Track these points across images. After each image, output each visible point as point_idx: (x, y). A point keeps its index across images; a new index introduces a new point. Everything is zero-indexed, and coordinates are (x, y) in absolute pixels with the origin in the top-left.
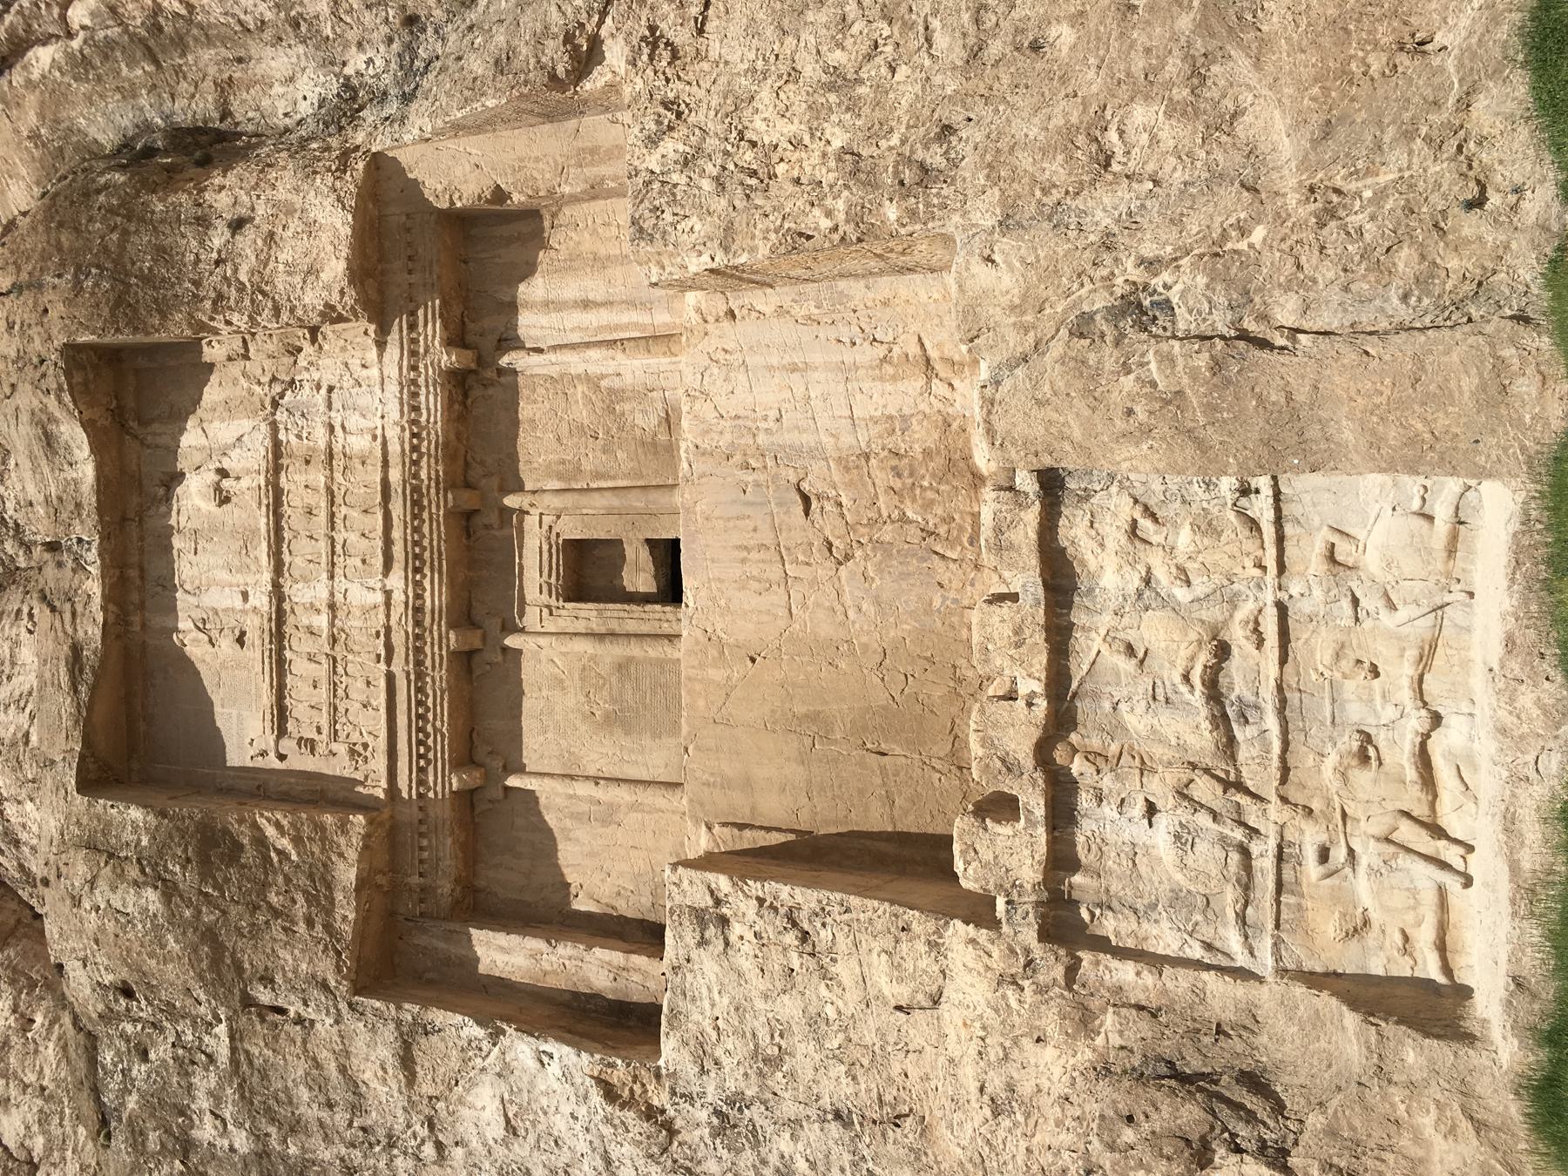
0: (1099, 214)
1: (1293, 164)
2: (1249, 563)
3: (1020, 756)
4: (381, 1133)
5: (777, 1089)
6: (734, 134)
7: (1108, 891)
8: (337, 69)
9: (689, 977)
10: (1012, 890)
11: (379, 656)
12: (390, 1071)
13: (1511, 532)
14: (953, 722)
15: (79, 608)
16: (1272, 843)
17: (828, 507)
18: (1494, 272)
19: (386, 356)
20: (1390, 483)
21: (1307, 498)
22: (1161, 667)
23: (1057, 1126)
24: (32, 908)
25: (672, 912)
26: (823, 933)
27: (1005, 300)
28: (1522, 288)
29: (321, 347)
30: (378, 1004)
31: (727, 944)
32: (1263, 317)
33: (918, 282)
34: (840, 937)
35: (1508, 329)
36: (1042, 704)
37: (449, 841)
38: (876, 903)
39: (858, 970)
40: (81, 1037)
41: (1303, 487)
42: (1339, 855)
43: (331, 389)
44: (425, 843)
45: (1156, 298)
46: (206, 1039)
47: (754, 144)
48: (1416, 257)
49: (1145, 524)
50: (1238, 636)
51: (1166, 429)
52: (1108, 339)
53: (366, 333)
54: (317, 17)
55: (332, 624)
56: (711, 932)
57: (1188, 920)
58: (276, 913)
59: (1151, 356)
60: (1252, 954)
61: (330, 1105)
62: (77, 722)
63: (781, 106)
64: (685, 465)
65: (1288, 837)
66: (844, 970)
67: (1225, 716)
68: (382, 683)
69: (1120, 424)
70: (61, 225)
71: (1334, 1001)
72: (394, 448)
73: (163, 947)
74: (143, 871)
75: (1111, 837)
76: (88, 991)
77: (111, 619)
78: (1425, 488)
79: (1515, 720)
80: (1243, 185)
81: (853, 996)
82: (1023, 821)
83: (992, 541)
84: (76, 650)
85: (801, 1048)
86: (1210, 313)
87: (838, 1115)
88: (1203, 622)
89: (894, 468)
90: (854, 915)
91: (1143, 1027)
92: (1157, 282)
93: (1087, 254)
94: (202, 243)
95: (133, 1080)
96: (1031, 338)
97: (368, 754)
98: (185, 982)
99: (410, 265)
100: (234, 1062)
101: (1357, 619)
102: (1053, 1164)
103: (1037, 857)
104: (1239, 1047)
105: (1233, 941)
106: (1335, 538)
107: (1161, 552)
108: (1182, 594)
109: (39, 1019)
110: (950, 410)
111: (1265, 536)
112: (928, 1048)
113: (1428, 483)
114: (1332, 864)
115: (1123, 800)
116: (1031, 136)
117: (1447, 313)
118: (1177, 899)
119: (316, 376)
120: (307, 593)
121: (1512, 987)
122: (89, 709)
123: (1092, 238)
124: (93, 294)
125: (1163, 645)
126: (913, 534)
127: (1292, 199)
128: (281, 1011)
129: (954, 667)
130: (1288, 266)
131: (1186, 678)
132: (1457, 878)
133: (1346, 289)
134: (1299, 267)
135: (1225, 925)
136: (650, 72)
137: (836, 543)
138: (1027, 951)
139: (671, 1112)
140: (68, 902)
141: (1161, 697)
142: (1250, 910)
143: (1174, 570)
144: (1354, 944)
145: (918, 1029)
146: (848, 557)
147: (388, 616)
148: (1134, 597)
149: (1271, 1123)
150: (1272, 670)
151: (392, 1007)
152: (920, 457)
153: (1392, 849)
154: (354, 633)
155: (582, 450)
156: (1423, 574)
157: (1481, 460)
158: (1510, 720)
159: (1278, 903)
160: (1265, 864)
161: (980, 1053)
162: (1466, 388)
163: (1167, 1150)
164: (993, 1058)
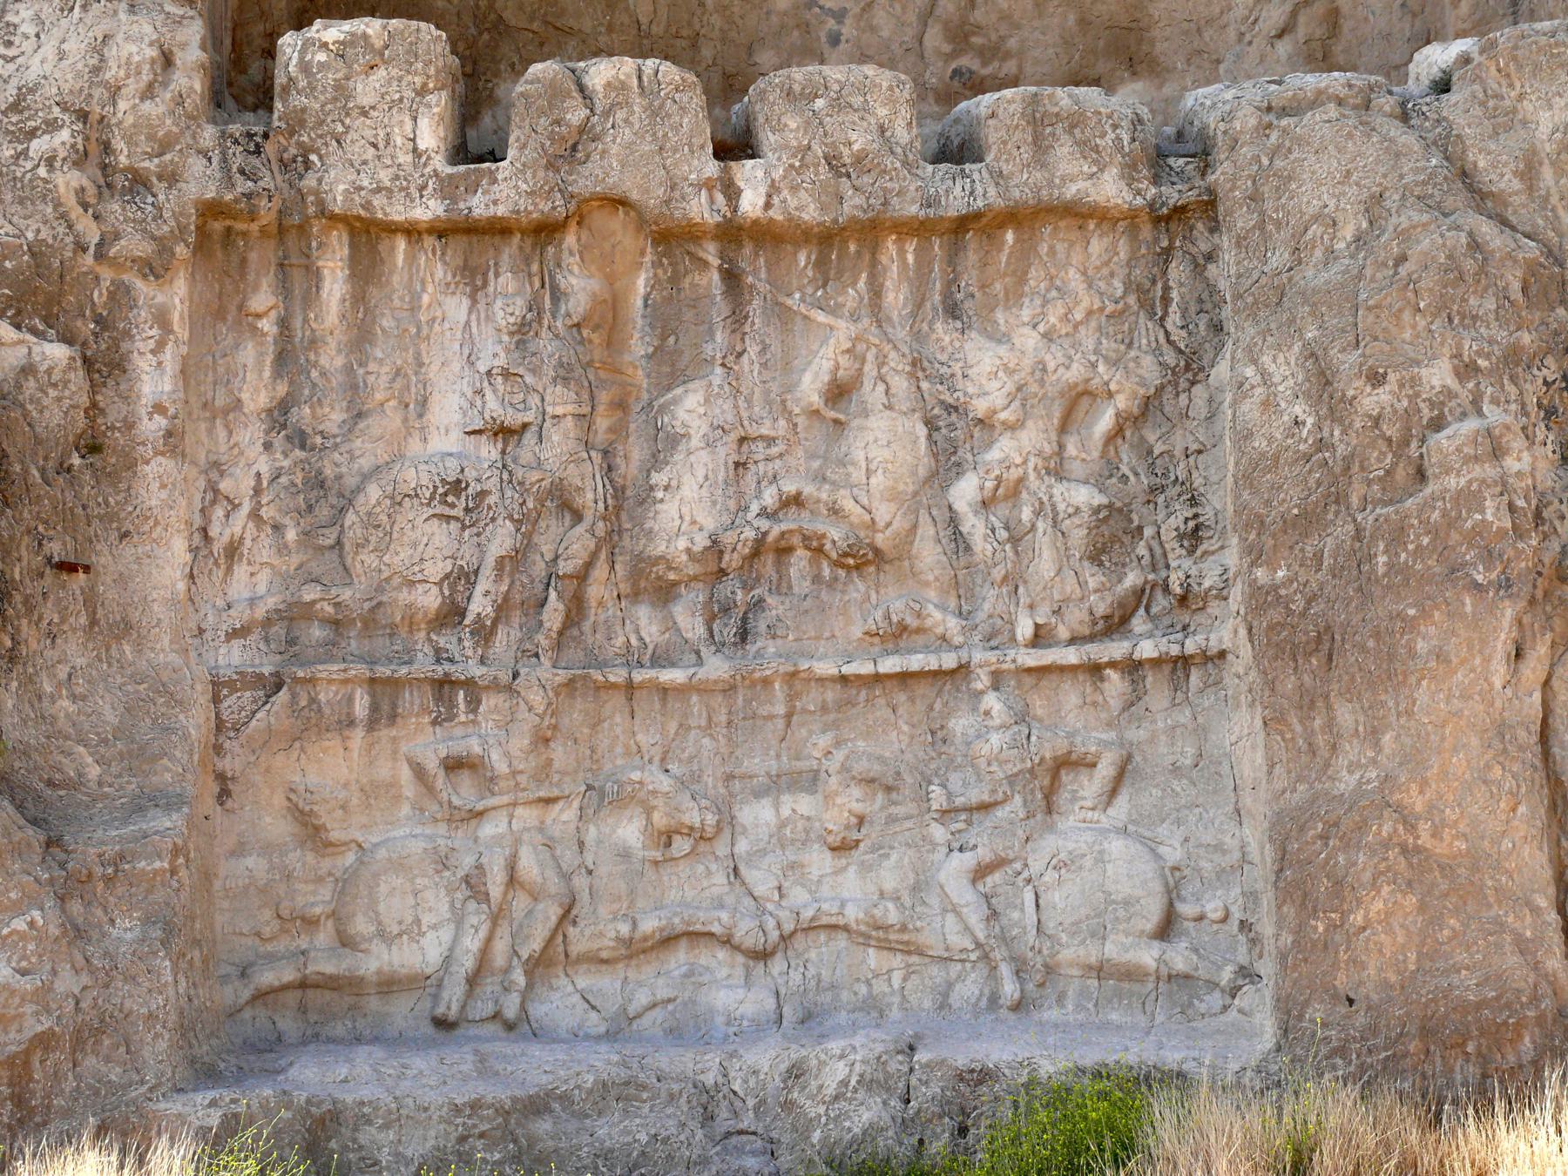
3: (594, 167)
21: (1184, 716)
42: (465, 793)
51: (1341, 450)
79: (830, 1090)
82: (450, 170)
106: (1106, 769)
143: (1015, 474)
156: (1050, 926)
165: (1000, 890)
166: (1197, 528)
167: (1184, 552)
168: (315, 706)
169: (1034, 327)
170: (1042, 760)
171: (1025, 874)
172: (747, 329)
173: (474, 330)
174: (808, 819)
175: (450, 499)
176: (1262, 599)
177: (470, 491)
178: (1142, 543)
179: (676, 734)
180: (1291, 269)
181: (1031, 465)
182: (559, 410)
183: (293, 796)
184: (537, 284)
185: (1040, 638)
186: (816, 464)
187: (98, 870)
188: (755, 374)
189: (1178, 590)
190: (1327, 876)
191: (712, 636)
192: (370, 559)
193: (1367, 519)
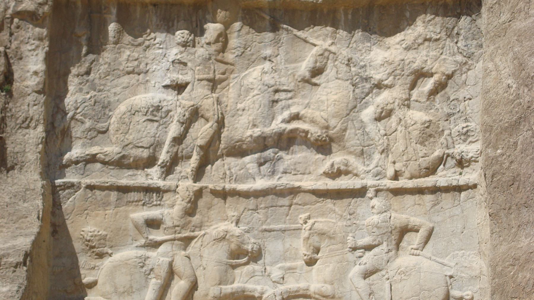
2: (398, 166)
16: (161, 183)
20: (474, 274)
21: (457, 211)
22: (304, 97)
49: (429, 84)
51: (527, 99)
57: (84, 115)
65: (166, 196)
67: (265, 148)
71: (36, 230)
75: (151, 53)
88: (345, 130)
101: (354, 249)
106: (423, 232)
107: (404, 97)
111: (422, 180)
114: (144, 229)
115: (185, 64)
125: (324, 98)
131: (296, 117)
135: (84, 145)
141: (277, 96)
142: (98, 165)
143: (389, 107)
150: (307, 183)
165: (375, 282)
166: (467, 131)
167: (461, 141)
168: (94, 197)
169: (401, 45)
170: (396, 228)
171: (386, 276)
172: (279, 45)
173: (168, 44)
174: (297, 249)
175: (155, 113)
176: (491, 162)
177: (163, 110)
178: (443, 137)
179: (243, 212)
180: (510, 21)
181: (396, 104)
182: (201, 76)
183: (82, 233)
184: (194, 25)
185: (396, 176)
188: (283, 64)
189: (458, 158)
190: (514, 282)
191: (260, 172)
192: (121, 137)
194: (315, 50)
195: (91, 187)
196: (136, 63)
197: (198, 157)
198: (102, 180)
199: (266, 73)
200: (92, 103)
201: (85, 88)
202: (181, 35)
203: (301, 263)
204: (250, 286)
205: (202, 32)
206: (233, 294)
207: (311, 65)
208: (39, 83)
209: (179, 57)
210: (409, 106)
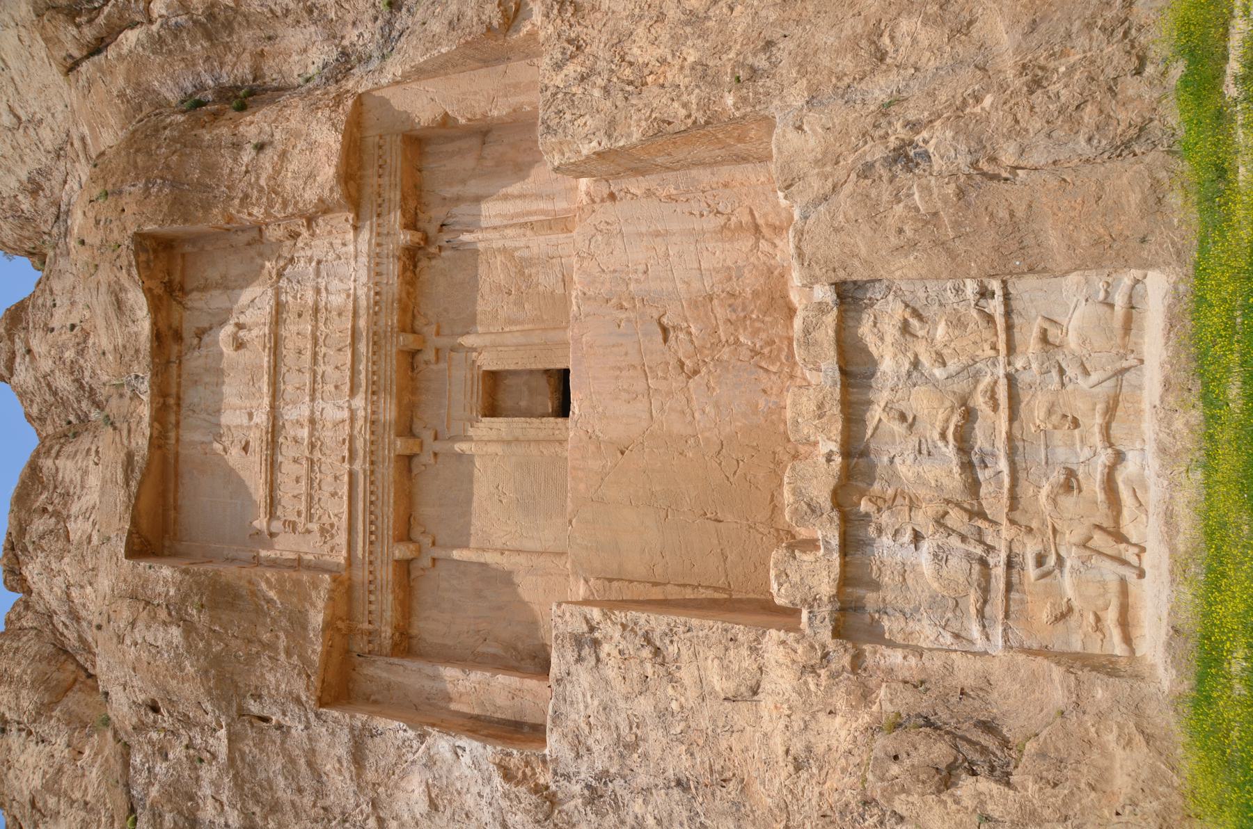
0: (877, 92)
1: (1010, 52)
2: (987, 347)
3: (821, 500)
4: (337, 811)
5: (634, 766)
6: (618, 57)
7: (884, 600)
8: (337, 41)
9: (569, 687)
10: (812, 602)
11: (344, 458)
12: (345, 764)
13: (1166, 304)
14: (773, 495)
15: (133, 426)
16: (1003, 556)
17: (682, 336)
18: (1151, 120)
19: (360, 240)
20: (1083, 281)
21: (1026, 296)
23: (842, 773)
24: (86, 670)
25: (557, 637)
26: (671, 648)
27: (810, 157)
28: (1170, 132)
29: (314, 231)
30: (336, 714)
31: (598, 660)
32: (993, 160)
33: (750, 169)
34: (684, 651)
35: (1161, 159)
36: (838, 459)
37: (390, 597)
38: (711, 623)
39: (696, 672)
40: (119, 746)
41: (1024, 287)
42: (1051, 561)
43: (319, 262)
44: (373, 598)
45: (918, 150)
46: (211, 741)
47: (631, 64)
48: (1096, 111)
49: (914, 322)
50: (980, 402)
51: (927, 243)
52: (885, 179)
53: (347, 220)
54: (325, 6)
55: (311, 435)
56: (586, 651)
57: (942, 617)
58: (266, 646)
59: (915, 188)
60: (988, 639)
61: (300, 791)
62: (128, 507)
63: (651, 37)
64: (575, 308)
65: (1016, 550)
66: (686, 675)
68: (346, 478)
69: (894, 241)
70: (138, 150)
71: (1046, 662)
72: (363, 302)
73: (182, 670)
74: (170, 614)
75: (887, 560)
76: (126, 709)
77: (156, 434)
78: (1107, 283)
79: (1171, 439)
80: (976, 66)
81: (692, 693)
82: (822, 551)
83: (802, 340)
84: (130, 456)
85: (652, 736)
86: (956, 158)
87: (679, 783)
88: (955, 393)
89: (730, 306)
90: (695, 633)
91: (909, 696)
92: (918, 139)
93: (869, 119)
94: (235, 160)
95: (156, 775)
96: (829, 184)
97: (334, 531)
98: (197, 696)
99: (381, 171)
100: (231, 760)
101: (1063, 385)
102: (839, 800)
103: (832, 576)
104: (977, 703)
105: (975, 631)
106: (1046, 325)
107: (925, 343)
108: (939, 373)
109: (87, 752)
110: (773, 262)
111: (999, 327)
112: (748, 728)
113: (1110, 280)
114: (1045, 568)
116: (829, 42)
117: (1119, 151)
118: (935, 602)
119: (309, 253)
120: (295, 413)
121: (1172, 632)
122: (137, 498)
123: (872, 108)
124: (157, 196)
125: (926, 411)
126: (745, 354)
127: (1010, 74)
128: (266, 720)
129: (774, 453)
130: (1009, 120)
131: (943, 436)
132: (1134, 571)
133: (1049, 136)
134: (1017, 122)
136: (559, 21)
137: (687, 362)
138: (824, 646)
139: (553, 787)
140: (115, 640)
141: (925, 452)
142: (987, 608)
143: (934, 355)
144: (1060, 626)
145: (741, 715)
146: (696, 372)
147: (352, 427)
148: (905, 377)
149: (999, 753)
150: (1003, 426)
151: (347, 716)
152: (750, 297)
153: (1088, 553)
154: (327, 441)
155: (499, 304)
157: (1145, 254)
158: (1168, 441)
159: (1007, 599)
160: (999, 572)
161: (787, 726)
162: (1132, 202)
163: (923, 777)
164: (796, 729)
182: (907, 518)
186: (929, 426)
187: (1074, 699)
189: (978, 296)
193: (951, 234)
194: (885, 420)
195: (1007, 616)
196: (895, 573)
197: (980, 521)
198: (1000, 605)
199: (904, 461)
200: (931, 611)
201: (918, 616)
202: (872, 532)
203: (1076, 432)
204: (1099, 477)
205: (867, 515)
206: (1106, 493)
207: (897, 422)
208: (913, 655)
209: (890, 536)
210: (932, 340)
